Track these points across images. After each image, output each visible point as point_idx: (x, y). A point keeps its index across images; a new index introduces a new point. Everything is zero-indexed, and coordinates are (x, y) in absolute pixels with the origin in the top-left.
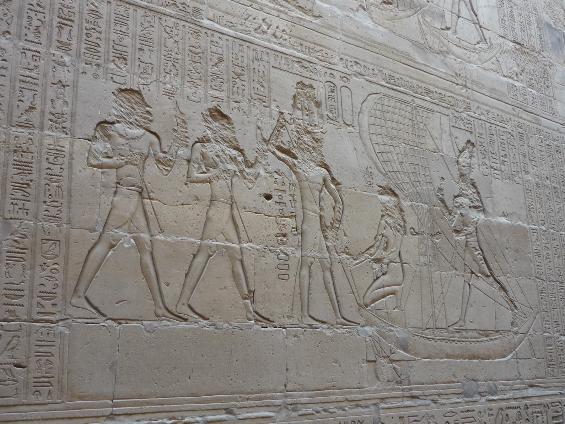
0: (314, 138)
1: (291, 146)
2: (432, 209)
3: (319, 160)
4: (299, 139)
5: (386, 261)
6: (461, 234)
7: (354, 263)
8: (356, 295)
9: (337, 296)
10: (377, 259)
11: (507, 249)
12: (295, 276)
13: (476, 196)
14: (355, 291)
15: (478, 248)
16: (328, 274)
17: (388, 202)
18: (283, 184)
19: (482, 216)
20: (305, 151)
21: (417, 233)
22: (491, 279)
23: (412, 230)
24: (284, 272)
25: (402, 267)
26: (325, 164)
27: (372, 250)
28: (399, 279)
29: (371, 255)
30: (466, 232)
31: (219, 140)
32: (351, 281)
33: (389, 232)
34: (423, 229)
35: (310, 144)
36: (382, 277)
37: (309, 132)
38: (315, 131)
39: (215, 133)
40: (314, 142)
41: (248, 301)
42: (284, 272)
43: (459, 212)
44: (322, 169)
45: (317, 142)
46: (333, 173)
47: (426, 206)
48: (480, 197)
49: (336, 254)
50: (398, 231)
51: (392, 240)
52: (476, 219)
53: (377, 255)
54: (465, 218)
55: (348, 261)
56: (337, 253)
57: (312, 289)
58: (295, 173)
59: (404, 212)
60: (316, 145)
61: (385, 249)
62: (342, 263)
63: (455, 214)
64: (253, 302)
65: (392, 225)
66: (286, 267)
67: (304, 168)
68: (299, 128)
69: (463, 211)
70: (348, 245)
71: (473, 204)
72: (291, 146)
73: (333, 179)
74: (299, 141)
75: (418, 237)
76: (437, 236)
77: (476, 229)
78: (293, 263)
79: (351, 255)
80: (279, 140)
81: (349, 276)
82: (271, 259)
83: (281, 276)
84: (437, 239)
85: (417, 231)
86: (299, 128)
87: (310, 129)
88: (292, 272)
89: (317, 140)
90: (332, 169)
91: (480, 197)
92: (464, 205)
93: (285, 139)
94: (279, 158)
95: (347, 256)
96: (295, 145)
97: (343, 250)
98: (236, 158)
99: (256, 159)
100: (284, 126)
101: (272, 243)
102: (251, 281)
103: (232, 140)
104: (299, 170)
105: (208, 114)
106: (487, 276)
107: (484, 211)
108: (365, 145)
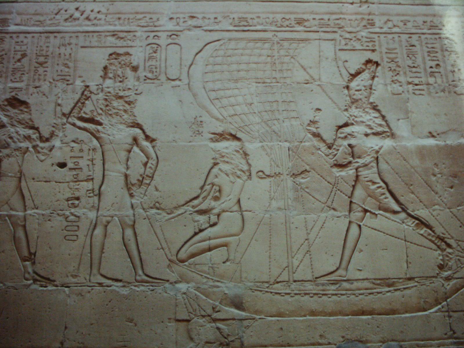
0: (126, 102)
1: (95, 114)
2: (297, 147)
3: (129, 121)
4: (107, 106)
5: (216, 211)
6: (349, 168)
7: (166, 218)
8: (167, 250)
9: (139, 252)
10: (202, 210)
11: (435, 175)
12: (86, 236)
13: (379, 121)
14: (164, 245)
15: (378, 180)
16: (129, 232)
17: (227, 148)
18: (81, 150)
19: (388, 143)
20: (114, 116)
21: (267, 176)
22: (403, 215)
23: (261, 174)
24: (72, 233)
25: (242, 215)
26: (138, 124)
27: (196, 202)
28: (235, 229)
29: (193, 207)
30: (357, 165)
31: (15, 123)
32: (161, 236)
33: (223, 180)
34: (277, 170)
35: (121, 108)
36: (209, 229)
37: (121, 97)
38: (127, 95)
39: (12, 119)
40: (127, 105)
41: (27, 263)
42: (72, 233)
43: (346, 143)
44: (133, 129)
45: (129, 104)
46: (146, 131)
47: (287, 144)
48: (386, 121)
49: (141, 211)
50: (239, 177)
51: (226, 189)
52: (377, 148)
53: (203, 207)
54: (355, 149)
55: (159, 216)
56: (144, 209)
57: (105, 247)
58: (97, 139)
59: (248, 155)
60: (127, 107)
61: (216, 199)
62: (149, 219)
63: (340, 146)
64: (34, 263)
65: (229, 172)
66: (76, 228)
67: (109, 132)
68: (107, 96)
69: (353, 142)
70: (160, 200)
71: (373, 131)
72: (95, 114)
73: (147, 138)
74: (108, 108)
75: (268, 180)
76: (303, 176)
77: (377, 159)
78: (84, 225)
79: (163, 210)
80: (82, 111)
81: (158, 231)
82: (58, 222)
83: (67, 238)
84: (303, 178)
85: (267, 173)
86: (107, 96)
87: (121, 94)
88: (81, 234)
89: (129, 103)
90: (145, 127)
91: (386, 121)
92: (356, 134)
93: (88, 109)
94: (80, 128)
95: (157, 211)
96: (100, 112)
97: (151, 205)
98: (29, 136)
99: (52, 134)
100: (90, 97)
101: (61, 207)
102: (32, 244)
103: (28, 121)
104: (102, 135)
105: (6, 103)
106: (395, 212)
107: (393, 136)
108: (195, 95)
